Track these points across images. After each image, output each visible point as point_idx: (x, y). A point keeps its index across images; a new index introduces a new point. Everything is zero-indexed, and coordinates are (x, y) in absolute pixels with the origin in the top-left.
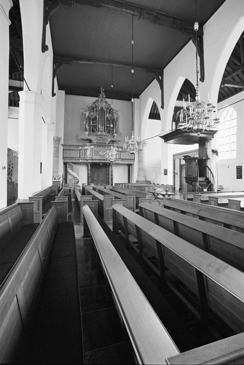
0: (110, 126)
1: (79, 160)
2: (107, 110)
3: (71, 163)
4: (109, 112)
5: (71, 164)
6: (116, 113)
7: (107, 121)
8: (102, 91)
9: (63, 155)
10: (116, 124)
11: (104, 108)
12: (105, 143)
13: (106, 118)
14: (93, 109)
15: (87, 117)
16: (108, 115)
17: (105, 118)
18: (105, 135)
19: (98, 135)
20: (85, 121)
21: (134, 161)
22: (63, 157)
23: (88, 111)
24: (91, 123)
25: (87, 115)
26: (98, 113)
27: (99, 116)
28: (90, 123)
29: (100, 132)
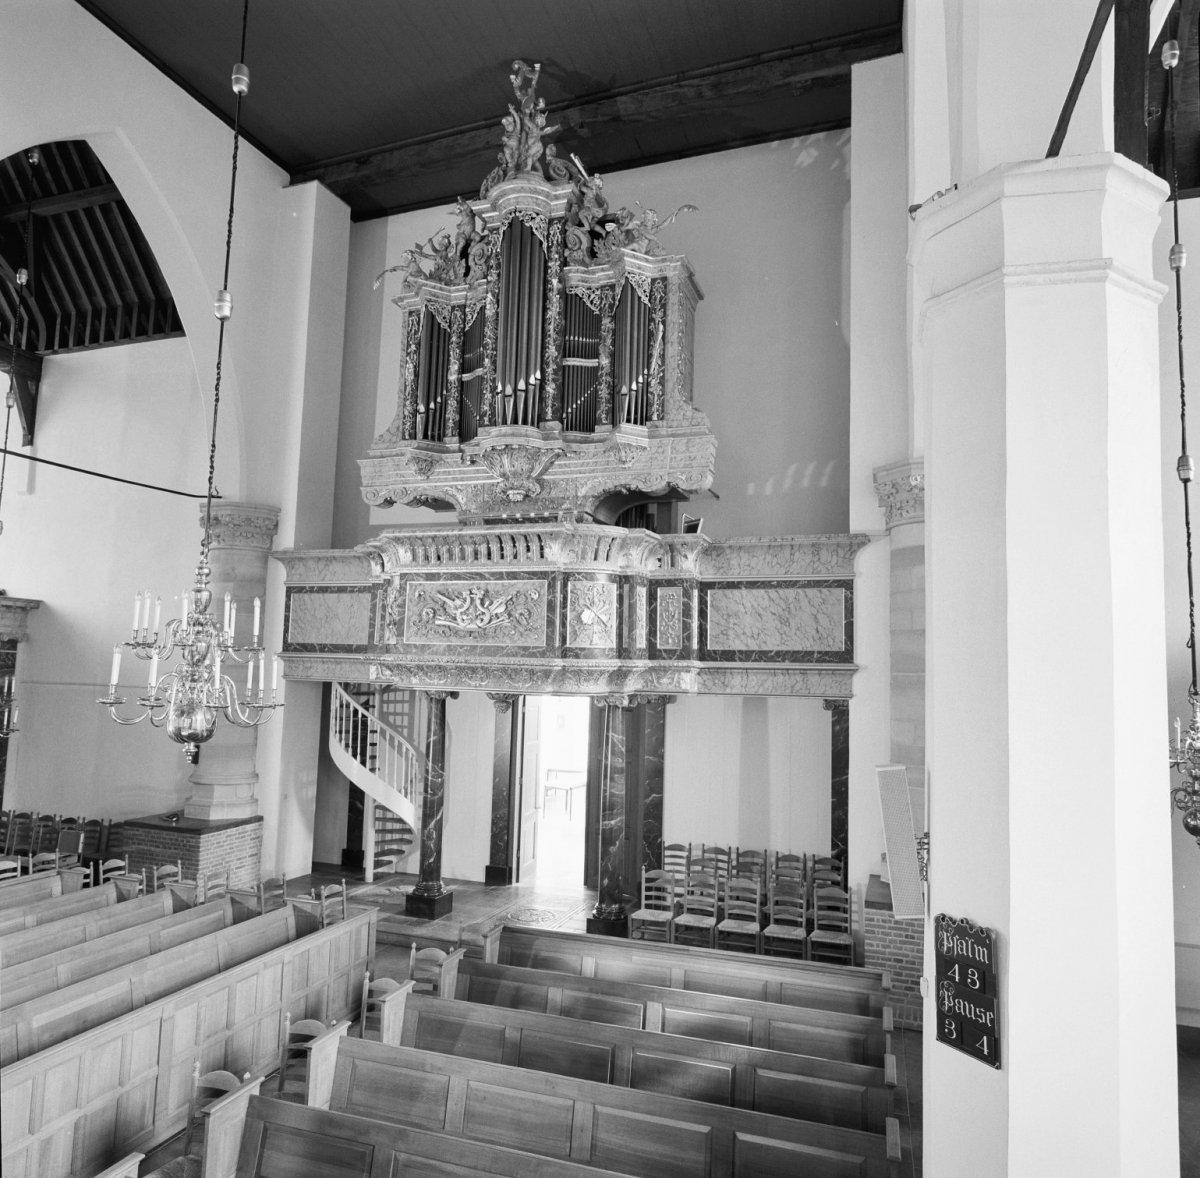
1: (369, 662)
2: (572, 230)
4: (593, 254)
7: (563, 332)
8: (527, 82)
9: (286, 631)
10: (651, 335)
11: (538, 227)
13: (555, 298)
14: (464, 254)
16: (586, 280)
17: (545, 309)
18: (536, 453)
20: (411, 366)
22: (287, 647)
26: (492, 278)
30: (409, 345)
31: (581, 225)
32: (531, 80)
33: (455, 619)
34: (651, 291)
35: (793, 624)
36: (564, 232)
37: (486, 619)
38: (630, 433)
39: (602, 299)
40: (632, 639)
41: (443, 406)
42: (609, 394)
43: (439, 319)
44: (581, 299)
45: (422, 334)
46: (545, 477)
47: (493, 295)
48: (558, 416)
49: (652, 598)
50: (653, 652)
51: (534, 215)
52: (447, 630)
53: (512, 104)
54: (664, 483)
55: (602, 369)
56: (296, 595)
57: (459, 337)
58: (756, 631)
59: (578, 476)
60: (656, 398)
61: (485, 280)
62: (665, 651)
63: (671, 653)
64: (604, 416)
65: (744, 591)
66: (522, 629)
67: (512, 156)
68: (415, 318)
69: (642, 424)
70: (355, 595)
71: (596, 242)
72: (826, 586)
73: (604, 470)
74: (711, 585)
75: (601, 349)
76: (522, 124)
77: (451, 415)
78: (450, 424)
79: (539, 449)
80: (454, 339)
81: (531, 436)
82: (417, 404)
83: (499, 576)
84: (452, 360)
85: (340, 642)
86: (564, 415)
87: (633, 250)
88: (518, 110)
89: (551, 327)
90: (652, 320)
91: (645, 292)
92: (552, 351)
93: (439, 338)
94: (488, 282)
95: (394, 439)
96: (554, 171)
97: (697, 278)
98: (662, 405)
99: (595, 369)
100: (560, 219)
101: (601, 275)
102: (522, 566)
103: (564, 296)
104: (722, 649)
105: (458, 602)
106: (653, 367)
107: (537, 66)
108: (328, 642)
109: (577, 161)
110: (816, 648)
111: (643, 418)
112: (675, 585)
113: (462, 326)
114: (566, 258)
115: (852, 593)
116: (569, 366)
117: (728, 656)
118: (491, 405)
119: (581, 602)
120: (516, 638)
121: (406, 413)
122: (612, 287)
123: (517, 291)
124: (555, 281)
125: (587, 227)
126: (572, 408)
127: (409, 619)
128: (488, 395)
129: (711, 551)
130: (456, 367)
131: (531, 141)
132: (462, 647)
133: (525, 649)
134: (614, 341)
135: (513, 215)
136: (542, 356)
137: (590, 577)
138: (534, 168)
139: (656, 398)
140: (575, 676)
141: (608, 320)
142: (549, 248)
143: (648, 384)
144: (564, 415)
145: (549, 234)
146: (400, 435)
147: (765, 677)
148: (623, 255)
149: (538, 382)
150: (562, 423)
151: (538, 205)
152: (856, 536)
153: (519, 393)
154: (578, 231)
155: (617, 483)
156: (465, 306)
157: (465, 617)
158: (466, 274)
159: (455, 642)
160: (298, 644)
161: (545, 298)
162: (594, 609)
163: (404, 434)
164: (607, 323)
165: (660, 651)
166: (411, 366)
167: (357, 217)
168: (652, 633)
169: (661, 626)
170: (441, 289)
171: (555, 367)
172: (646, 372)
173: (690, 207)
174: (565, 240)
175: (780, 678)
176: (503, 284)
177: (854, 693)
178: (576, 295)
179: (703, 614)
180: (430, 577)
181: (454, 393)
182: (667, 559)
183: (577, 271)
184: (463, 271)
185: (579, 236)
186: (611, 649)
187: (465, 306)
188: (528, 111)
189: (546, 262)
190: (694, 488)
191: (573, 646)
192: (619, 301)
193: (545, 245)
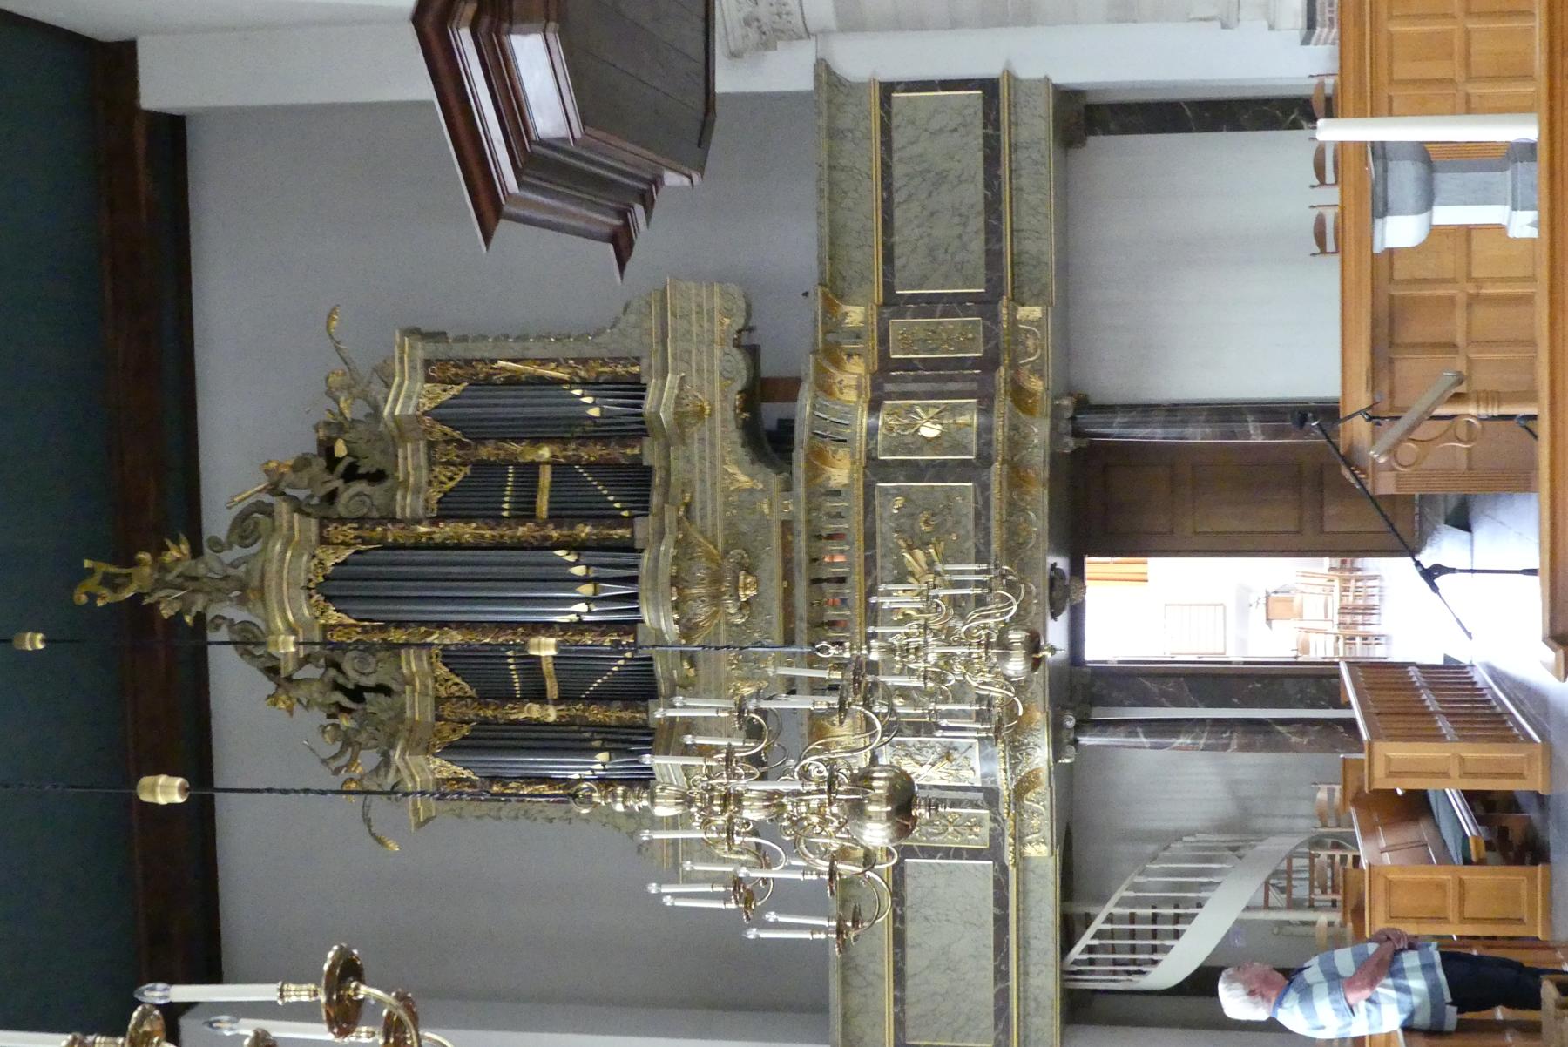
0: (554, 464)
1: (1021, 860)
2: (342, 506)
3: (1076, 953)
4: (377, 477)
5: (1090, 949)
6: (376, 388)
8: (110, 582)
10: (513, 381)
11: (331, 558)
12: (787, 526)
13: (445, 530)
14: (357, 694)
15: (466, 774)
17: (459, 547)
18: (684, 545)
19: (688, 629)
21: (1010, 75)
23: (386, 761)
24: (534, 711)
25: (441, 768)
26: (396, 636)
27: (441, 625)
28: (540, 724)
29: (646, 615)
34: (443, 382)
35: (946, 166)
36: (342, 521)
38: (660, 401)
44: (445, 495)
48: (629, 523)
51: (316, 561)
56: (910, 1032)
57: (487, 705)
58: (957, 220)
60: (606, 369)
63: (989, 335)
64: (629, 451)
65: (897, 238)
69: (644, 390)
70: (909, 914)
71: (362, 471)
72: (890, 119)
73: (713, 446)
74: (888, 287)
75: (529, 458)
78: (626, 715)
80: (489, 713)
81: (656, 559)
83: (870, 562)
85: (991, 942)
89: (488, 533)
90: (488, 381)
97: (424, 329)
98: (616, 360)
100: (322, 526)
101: (410, 461)
102: (853, 525)
104: (983, 270)
106: (554, 374)
107: (87, 564)
108: (990, 964)
110: (979, 131)
111: (634, 388)
114: (382, 518)
115: (899, 83)
116: (550, 509)
117: (993, 258)
119: (909, 440)
120: (962, 532)
122: (431, 445)
125: (339, 483)
130: (535, 707)
133: (978, 515)
134: (514, 440)
137: (872, 432)
139: (606, 369)
144: (625, 513)
145: (343, 543)
147: (1024, 209)
148: (392, 413)
152: (817, 76)
154: (344, 498)
155: (732, 426)
160: (996, 1025)
161: (443, 546)
164: (486, 452)
165: (985, 352)
171: (551, 526)
173: (330, 317)
175: (1024, 182)
177: (1040, 75)
178: (439, 502)
184: (382, 698)
185: (351, 496)
187: (438, 701)
190: (743, 306)
192: (455, 429)
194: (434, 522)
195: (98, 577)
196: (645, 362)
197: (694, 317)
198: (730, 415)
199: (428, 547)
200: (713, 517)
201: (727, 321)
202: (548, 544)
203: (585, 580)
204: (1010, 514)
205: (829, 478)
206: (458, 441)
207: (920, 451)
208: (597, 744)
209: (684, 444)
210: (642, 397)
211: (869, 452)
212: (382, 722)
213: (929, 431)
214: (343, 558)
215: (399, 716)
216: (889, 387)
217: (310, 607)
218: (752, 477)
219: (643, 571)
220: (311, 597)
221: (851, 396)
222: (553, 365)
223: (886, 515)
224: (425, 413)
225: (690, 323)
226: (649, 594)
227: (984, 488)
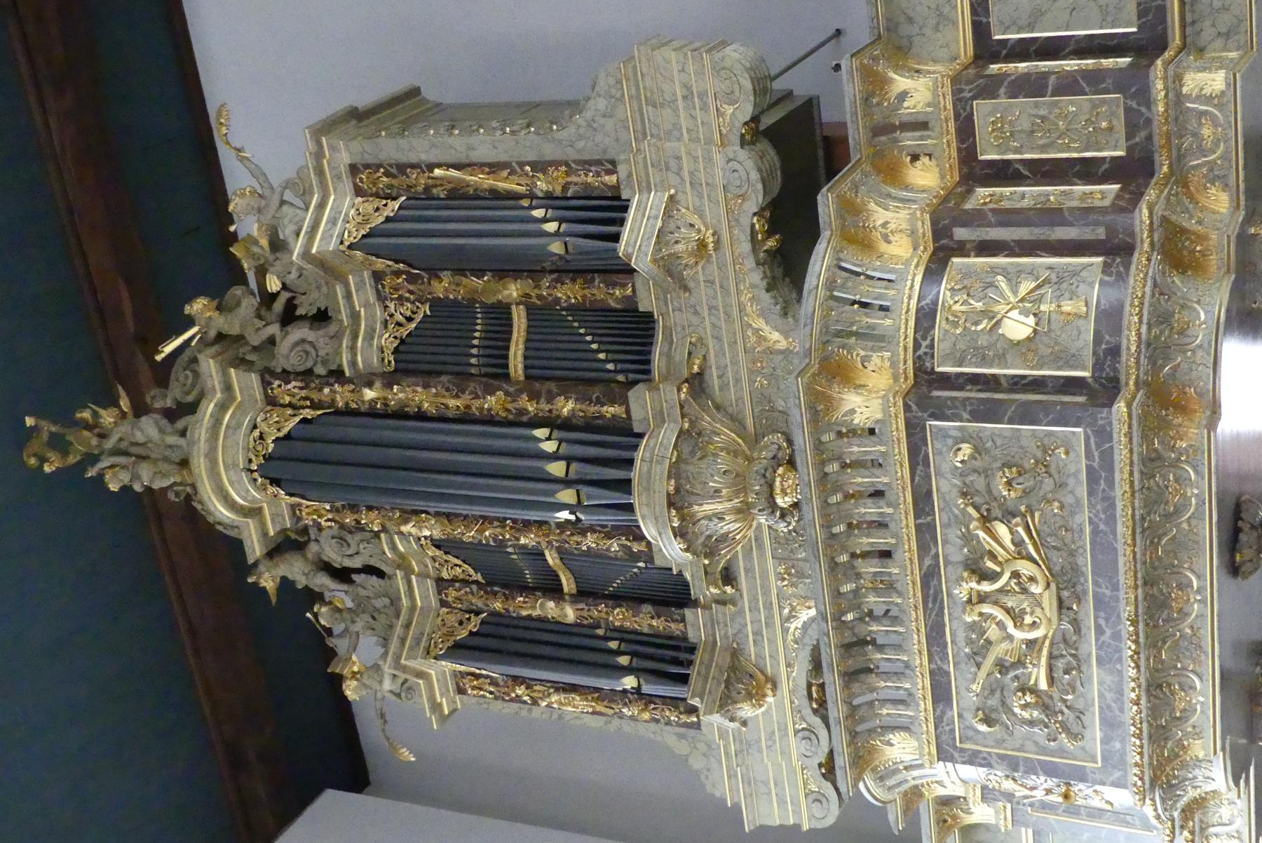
0: (525, 300)
4: (322, 317)
7: (462, 378)
10: (458, 194)
13: (399, 394)
16: (370, 330)
17: (421, 416)
18: (691, 438)
24: (550, 608)
28: (558, 627)
30: (518, 699)
31: (272, 341)
32: (52, 434)
33: (1030, 643)
36: (286, 376)
37: (1025, 568)
38: (636, 240)
39: (400, 298)
40: (1086, 213)
41: (622, 634)
42: (573, 280)
43: (462, 634)
44: (402, 342)
45: (494, 671)
46: (749, 422)
47: (406, 522)
48: (618, 395)
49: (1003, 173)
50: (1133, 172)
51: (256, 433)
52: (1060, 664)
53: (85, 470)
54: (743, 154)
55: (527, 296)
59: (740, 347)
60: (573, 179)
61: (382, 535)
62: (1129, 136)
63: (1136, 123)
66: (1048, 484)
67: (164, 476)
68: (467, 683)
69: (625, 209)
74: (981, 31)
76: (117, 452)
77: (646, 621)
79: (681, 433)
80: (498, 606)
82: (625, 691)
83: (926, 534)
84: (537, 612)
86: (621, 378)
87: (298, 235)
88: (92, 459)
89: (452, 403)
90: (427, 193)
91: (377, 209)
92: (492, 402)
93: (530, 641)
94: (384, 529)
95: (702, 747)
96: (188, 393)
97: (363, 101)
98: (587, 164)
99: (531, 311)
100: (266, 384)
102: (898, 475)
103: (398, 375)
105: (993, 632)
107: (29, 421)
109: (169, 348)
111: (609, 210)
112: (969, 119)
113: (474, 587)
116: (526, 367)
118: (609, 536)
119: (983, 341)
121: (646, 716)
122: (378, 277)
123: (460, 479)
124: (369, 394)
125: (274, 329)
126: (607, 361)
127: (1044, 751)
128: (590, 541)
129: (895, 42)
131: (140, 437)
132: (1099, 631)
135: (256, 475)
136: (511, 424)
137: (926, 317)
138: (183, 433)
139: (573, 179)
140: (1167, 359)
141: (435, 283)
142: (314, 406)
143: (549, 196)
144: (621, 378)
145: (290, 405)
146: (692, 732)
148: (306, 254)
149: (556, 434)
150: (636, 383)
151: (239, 426)
153: (572, 475)
154: (284, 347)
155: (750, 262)
156: (439, 581)
157: (1028, 620)
158: (380, 574)
159: (1090, 646)
161: (400, 414)
162: (1001, 308)
163: (686, 725)
164: (442, 287)
165: (1130, 149)
166: (554, 698)
167: (353, 773)
168: (1087, 171)
169: (1069, 149)
170: (407, 626)
171: (525, 397)
172: (525, 203)
174: (298, 374)
176: (383, 500)
178: (396, 351)
179: (1051, 49)
180: (941, 694)
181: (599, 611)
182: (909, 140)
183: (353, 348)
184: (374, 580)
185: (292, 345)
186: (1106, 268)
187: (439, 581)
188: (94, 441)
189: (338, 413)
191: (1090, 362)
192: (397, 262)
193: (308, 413)
194: (390, 379)
195: (45, 436)
196: (623, 170)
197: (680, 102)
198: (746, 246)
199: (385, 415)
200: (735, 383)
201: (729, 110)
202: (525, 419)
203: (566, 482)
204: (1147, 475)
205: (853, 411)
206: (407, 273)
207: (1001, 359)
208: (624, 660)
209: (686, 288)
210: (622, 222)
211: (918, 360)
212: (378, 610)
213: (1018, 327)
214: (285, 431)
215: (395, 601)
216: (961, 233)
217: (257, 489)
218: (786, 334)
219: (635, 474)
220: (255, 480)
221: (900, 248)
222: (505, 173)
223: (945, 467)
224: (350, 247)
225: (676, 111)
226: (645, 510)
227: (1103, 435)
